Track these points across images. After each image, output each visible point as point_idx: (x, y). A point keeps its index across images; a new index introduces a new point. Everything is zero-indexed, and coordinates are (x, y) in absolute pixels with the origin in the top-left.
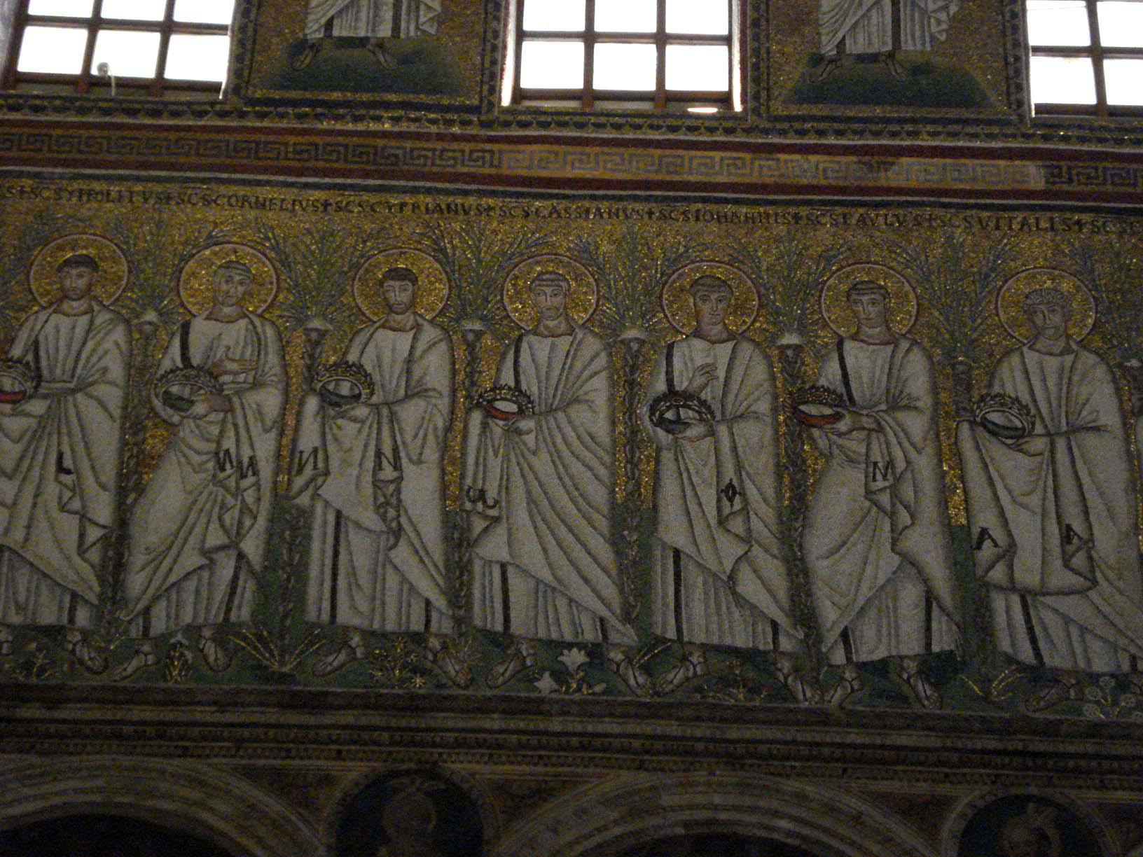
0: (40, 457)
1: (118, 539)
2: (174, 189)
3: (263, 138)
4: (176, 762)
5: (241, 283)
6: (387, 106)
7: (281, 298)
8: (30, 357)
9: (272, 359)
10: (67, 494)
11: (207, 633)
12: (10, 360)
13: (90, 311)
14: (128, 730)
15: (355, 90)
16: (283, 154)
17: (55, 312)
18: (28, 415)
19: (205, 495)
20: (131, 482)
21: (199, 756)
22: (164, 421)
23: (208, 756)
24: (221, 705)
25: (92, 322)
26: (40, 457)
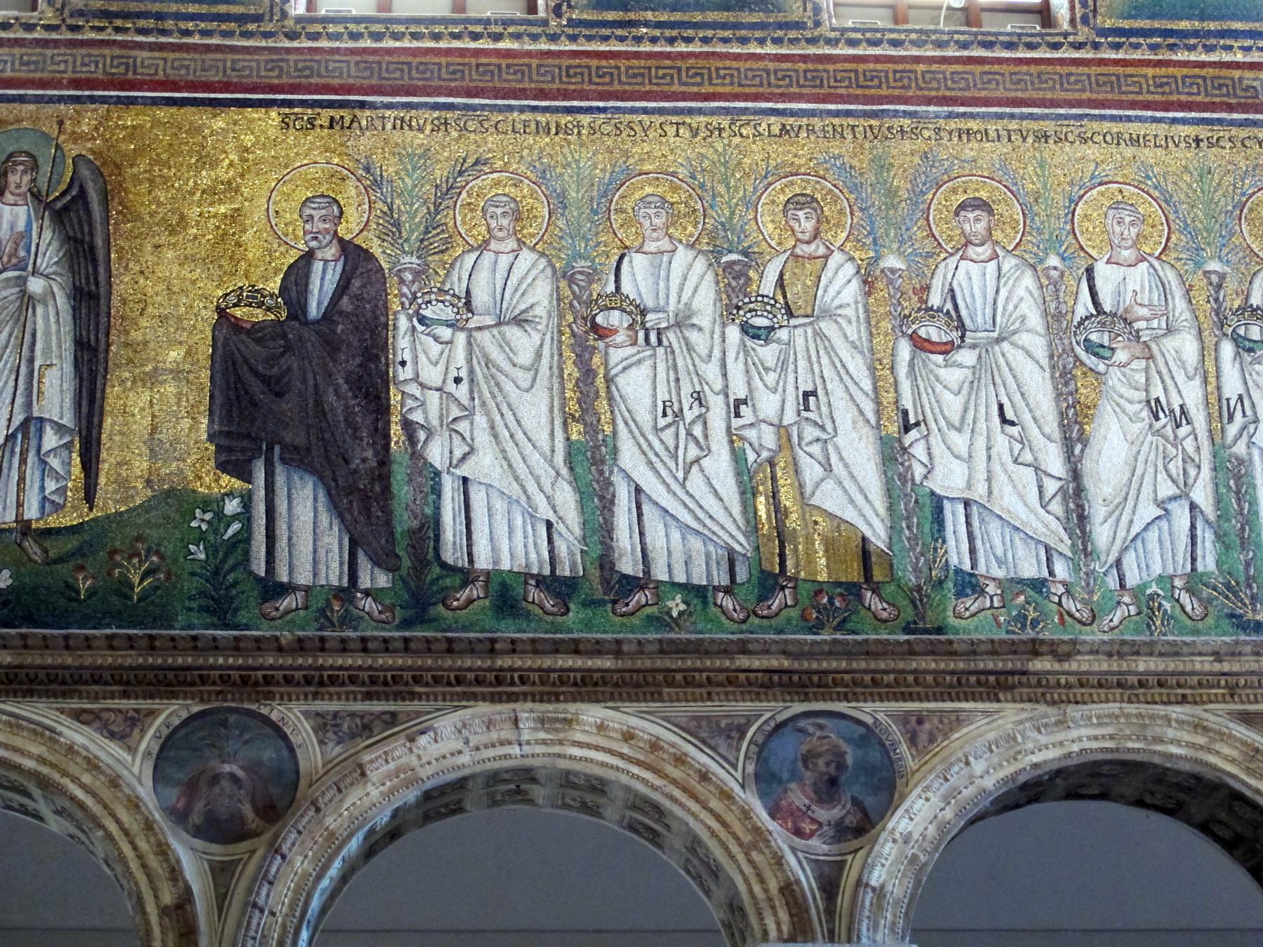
0: (982, 409)
1: (1076, 490)
2: (1049, 126)
3: (1120, 70)
4: (1178, 709)
5: (1132, 224)
6: (1235, 34)
7: (1174, 238)
8: (949, 306)
9: (1180, 304)
10: (1018, 446)
11: (1178, 583)
12: (931, 309)
13: (995, 256)
14: (1133, 679)
15: (1202, 18)
16: (1144, 86)
17: (962, 258)
18: (960, 366)
19: (1146, 445)
20: (1074, 432)
21: (1196, 703)
22: (1091, 369)
23: (1204, 703)
24: (1217, 656)
25: (999, 269)
26: (982, 409)
